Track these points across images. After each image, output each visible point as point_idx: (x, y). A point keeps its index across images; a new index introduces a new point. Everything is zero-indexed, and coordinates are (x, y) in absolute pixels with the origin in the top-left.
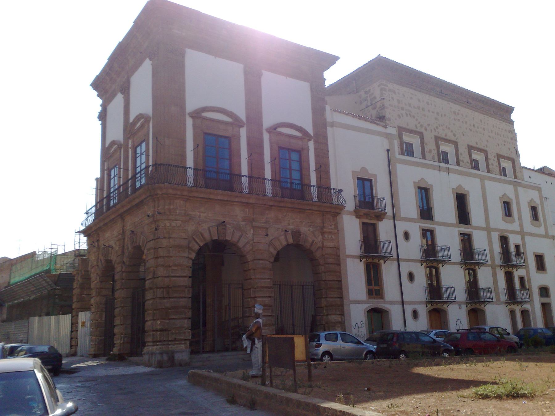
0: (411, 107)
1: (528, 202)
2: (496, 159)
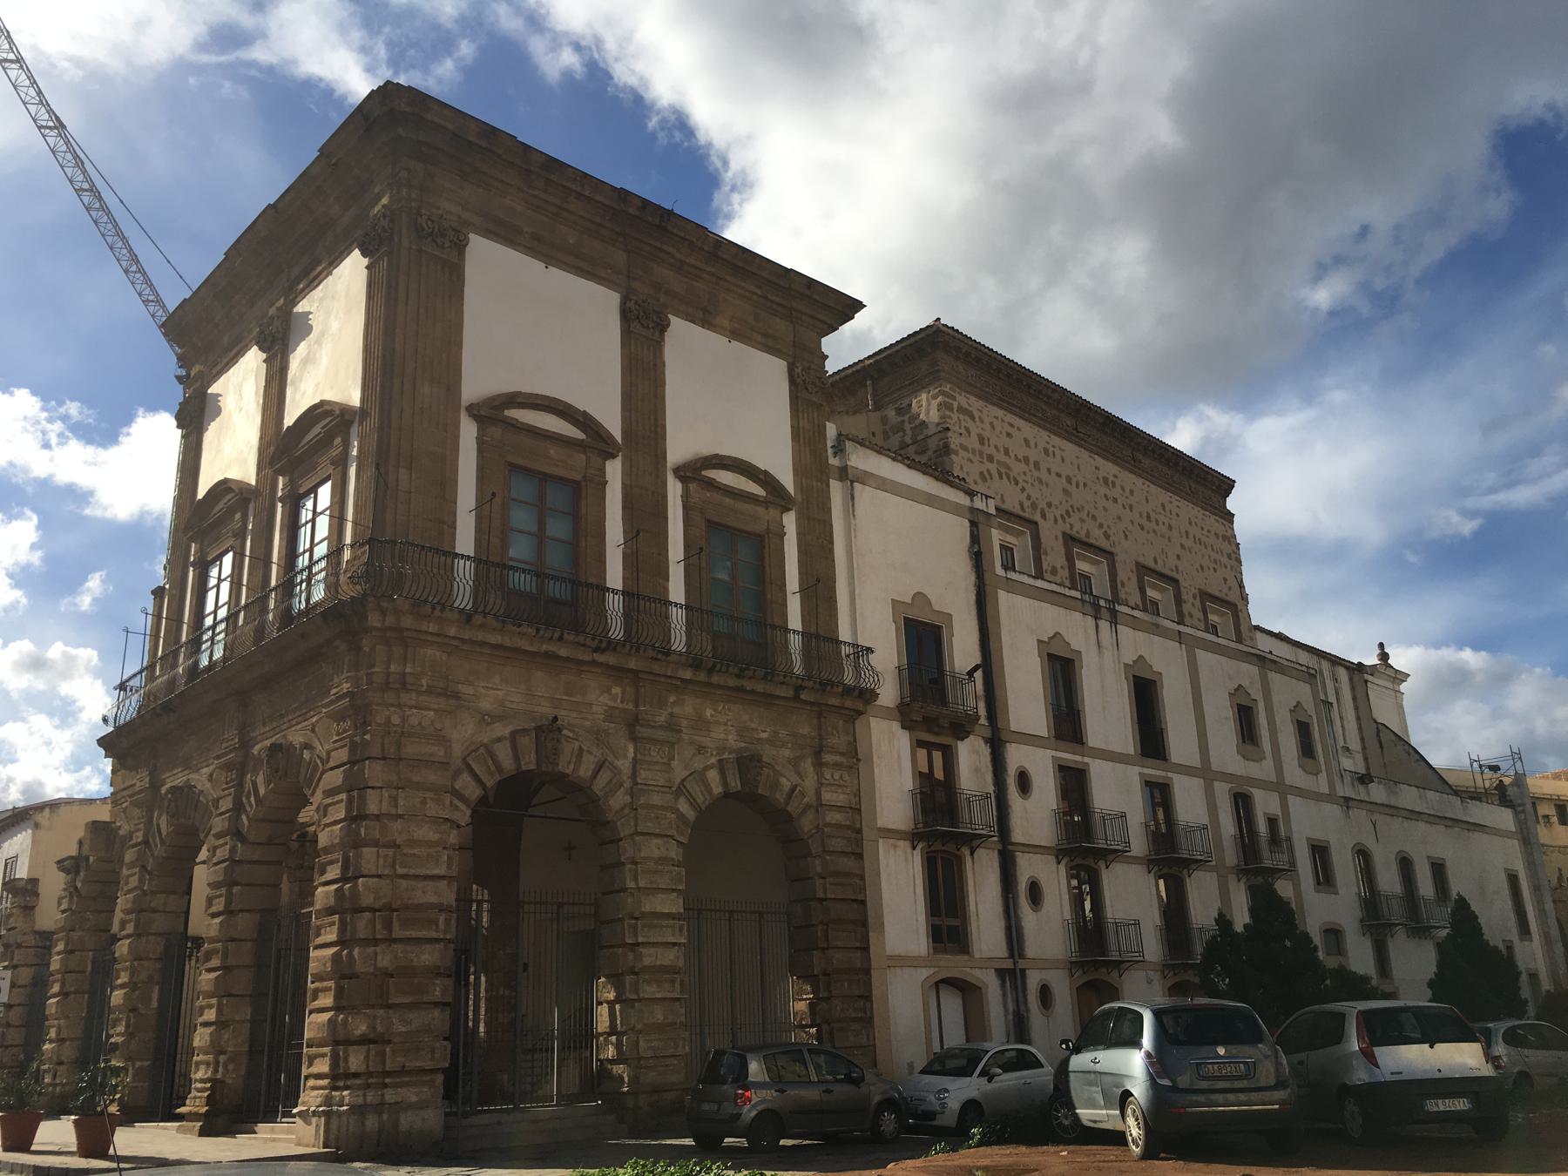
0: (1010, 457)
1: (1290, 710)
2: (1198, 603)
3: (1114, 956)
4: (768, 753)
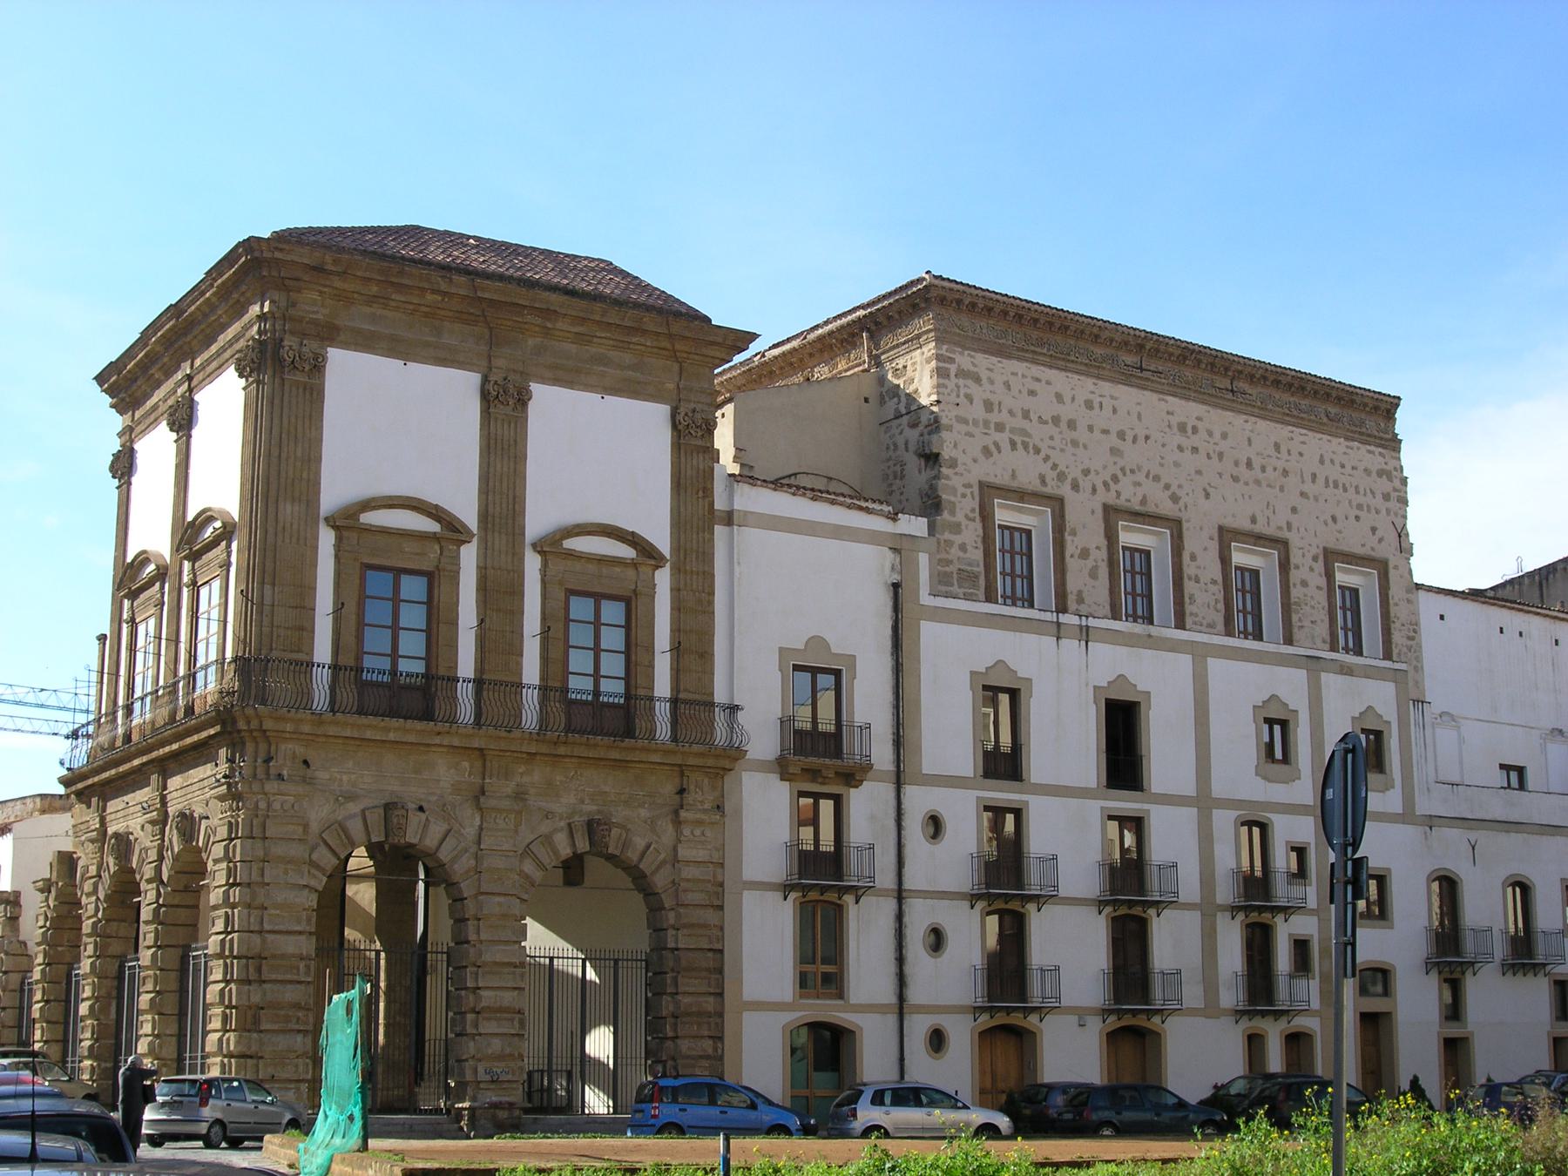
0: (1031, 421)
2: (1319, 566)
3: (1035, 1002)
4: (619, 814)
